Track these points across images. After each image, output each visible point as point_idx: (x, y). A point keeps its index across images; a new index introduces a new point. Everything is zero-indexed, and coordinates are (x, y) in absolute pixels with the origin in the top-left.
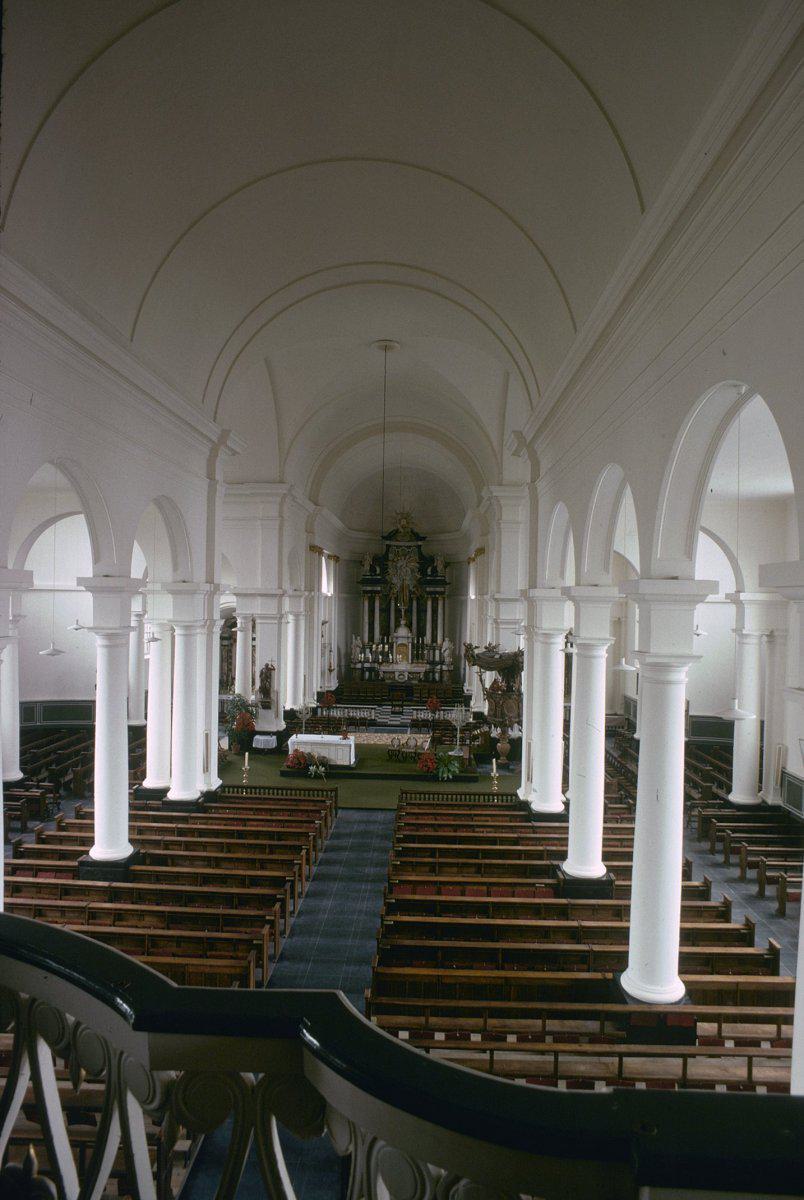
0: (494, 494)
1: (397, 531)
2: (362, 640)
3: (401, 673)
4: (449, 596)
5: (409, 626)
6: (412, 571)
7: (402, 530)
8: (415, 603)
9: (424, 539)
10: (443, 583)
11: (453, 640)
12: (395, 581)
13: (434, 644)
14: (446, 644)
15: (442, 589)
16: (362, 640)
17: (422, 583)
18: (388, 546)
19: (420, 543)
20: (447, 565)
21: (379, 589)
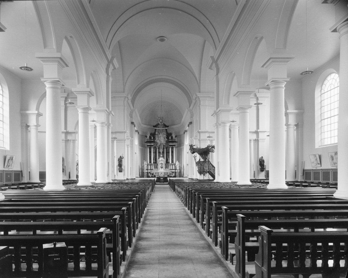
0: (198, 96)
1: (158, 124)
2: (147, 162)
3: (161, 173)
4: (177, 147)
5: (163, 157)
6: (164, 138)
7: (160, 123)
8: (165, 150)
9: (168, 127)
10: (175, 142)
11: (179, 162)
12: (158, 141)
13: (173, 163)
14: (177, 163)
15: (175, 144)
16: (147, 162)
17: (168, 142)
18: (156, 130)
19: (166, 128)
20: (176, 136)
21: (153, 144)
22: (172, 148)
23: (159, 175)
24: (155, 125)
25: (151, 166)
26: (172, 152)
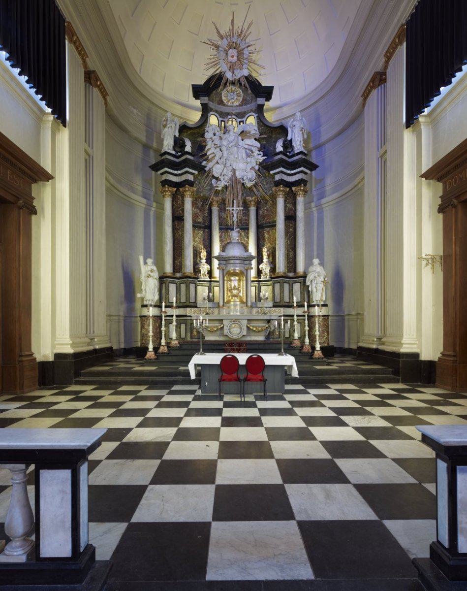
7: (229, 75)
12: (217, 170)
16: (159, 263)
17: (265, 167)
19: (260, 101)
22: (291, 199)
23: (222, 328)
24: (201, 82)
25: (183, 287)
26: (291, 218)
